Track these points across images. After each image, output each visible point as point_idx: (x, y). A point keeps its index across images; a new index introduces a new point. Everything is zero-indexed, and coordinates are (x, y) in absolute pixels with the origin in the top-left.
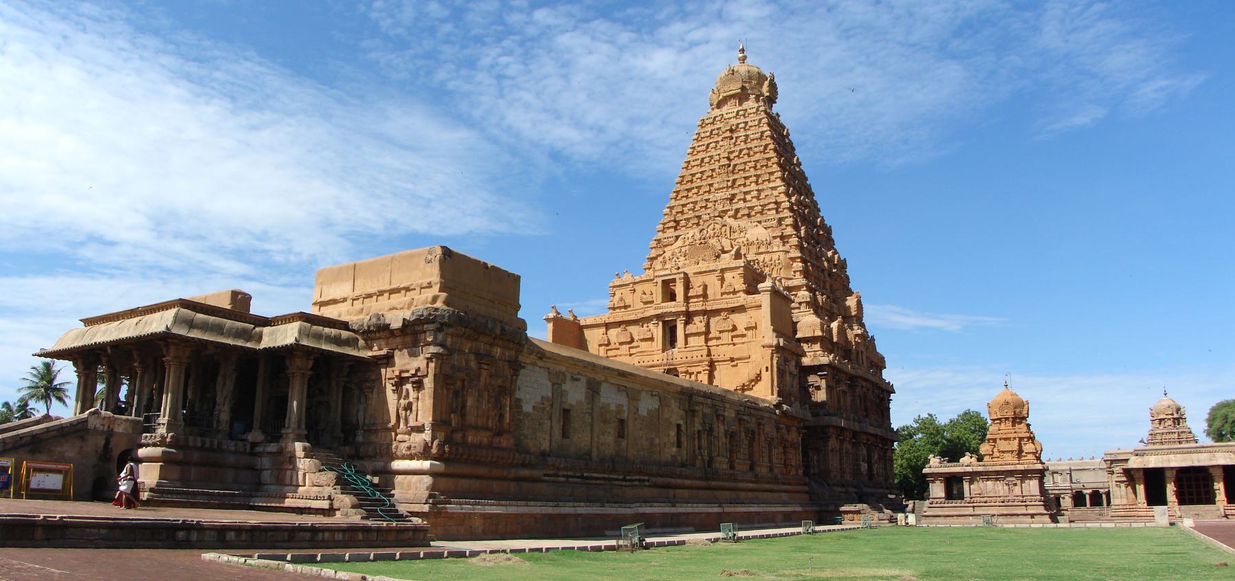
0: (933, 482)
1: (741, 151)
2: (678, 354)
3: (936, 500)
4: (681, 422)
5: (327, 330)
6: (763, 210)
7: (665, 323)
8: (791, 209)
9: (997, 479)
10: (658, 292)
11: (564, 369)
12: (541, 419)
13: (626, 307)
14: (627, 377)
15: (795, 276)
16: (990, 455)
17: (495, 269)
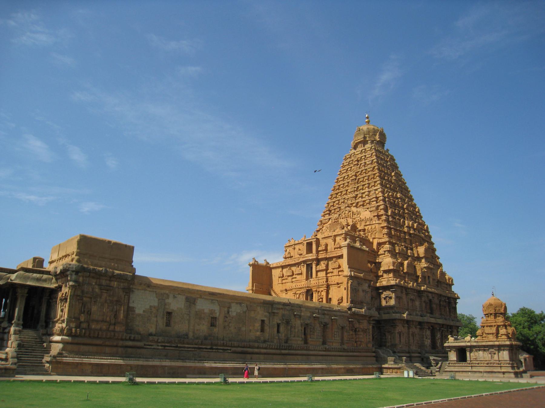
0: (450, 351)
1: (362, 171)
2: (313, 282)
3: (451, 362)
4: (265, 319)
5: (35, 275)
6: (370, 202)
7: (308, 265)
8: (384, 200)
9: (484, 350)
10: (305, 247)
11: (167, 292)
12: (149, 317)
13: (291, 257)
14: (216, 295)
15: (384, 236)
16: (481, 336)
17: (116, 244)
